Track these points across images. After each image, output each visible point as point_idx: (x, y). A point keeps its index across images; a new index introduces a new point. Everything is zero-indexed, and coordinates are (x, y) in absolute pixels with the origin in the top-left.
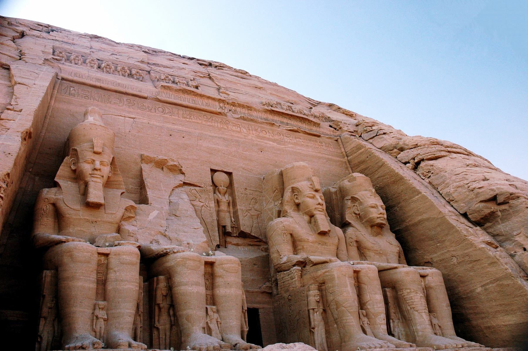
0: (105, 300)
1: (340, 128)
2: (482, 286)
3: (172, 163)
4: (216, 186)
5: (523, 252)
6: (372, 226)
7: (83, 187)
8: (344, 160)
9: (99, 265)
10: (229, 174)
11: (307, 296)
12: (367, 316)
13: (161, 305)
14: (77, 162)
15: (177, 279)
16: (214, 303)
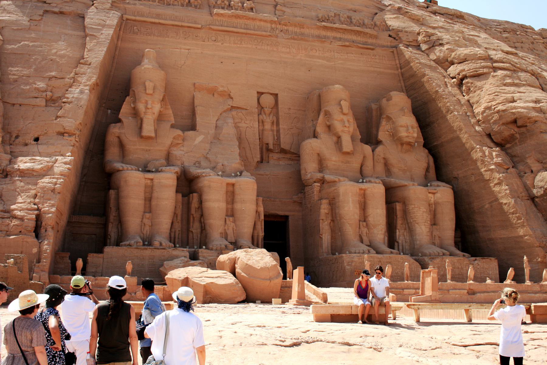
0: (150, 212)
1: (400, 38)
2: (489, 203)
3: (221, 89)
4: (263, 108)
5: (530, 174)
6: (402, 144)
7: (139, 122)
8: (396, 72)
9: (146, 186)
10: (276, 95)
11: (320, 208)
12: (367, 225)
13: (195, 216)
14: (134, 102)
15: (205, 197)
16: (232, 215)
